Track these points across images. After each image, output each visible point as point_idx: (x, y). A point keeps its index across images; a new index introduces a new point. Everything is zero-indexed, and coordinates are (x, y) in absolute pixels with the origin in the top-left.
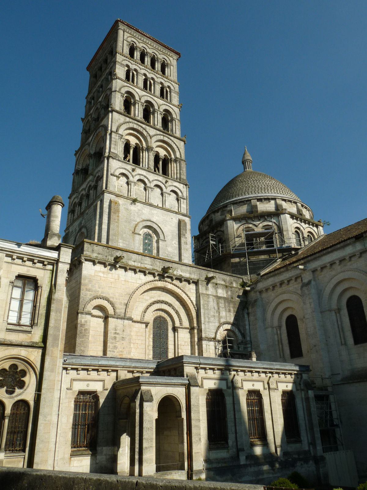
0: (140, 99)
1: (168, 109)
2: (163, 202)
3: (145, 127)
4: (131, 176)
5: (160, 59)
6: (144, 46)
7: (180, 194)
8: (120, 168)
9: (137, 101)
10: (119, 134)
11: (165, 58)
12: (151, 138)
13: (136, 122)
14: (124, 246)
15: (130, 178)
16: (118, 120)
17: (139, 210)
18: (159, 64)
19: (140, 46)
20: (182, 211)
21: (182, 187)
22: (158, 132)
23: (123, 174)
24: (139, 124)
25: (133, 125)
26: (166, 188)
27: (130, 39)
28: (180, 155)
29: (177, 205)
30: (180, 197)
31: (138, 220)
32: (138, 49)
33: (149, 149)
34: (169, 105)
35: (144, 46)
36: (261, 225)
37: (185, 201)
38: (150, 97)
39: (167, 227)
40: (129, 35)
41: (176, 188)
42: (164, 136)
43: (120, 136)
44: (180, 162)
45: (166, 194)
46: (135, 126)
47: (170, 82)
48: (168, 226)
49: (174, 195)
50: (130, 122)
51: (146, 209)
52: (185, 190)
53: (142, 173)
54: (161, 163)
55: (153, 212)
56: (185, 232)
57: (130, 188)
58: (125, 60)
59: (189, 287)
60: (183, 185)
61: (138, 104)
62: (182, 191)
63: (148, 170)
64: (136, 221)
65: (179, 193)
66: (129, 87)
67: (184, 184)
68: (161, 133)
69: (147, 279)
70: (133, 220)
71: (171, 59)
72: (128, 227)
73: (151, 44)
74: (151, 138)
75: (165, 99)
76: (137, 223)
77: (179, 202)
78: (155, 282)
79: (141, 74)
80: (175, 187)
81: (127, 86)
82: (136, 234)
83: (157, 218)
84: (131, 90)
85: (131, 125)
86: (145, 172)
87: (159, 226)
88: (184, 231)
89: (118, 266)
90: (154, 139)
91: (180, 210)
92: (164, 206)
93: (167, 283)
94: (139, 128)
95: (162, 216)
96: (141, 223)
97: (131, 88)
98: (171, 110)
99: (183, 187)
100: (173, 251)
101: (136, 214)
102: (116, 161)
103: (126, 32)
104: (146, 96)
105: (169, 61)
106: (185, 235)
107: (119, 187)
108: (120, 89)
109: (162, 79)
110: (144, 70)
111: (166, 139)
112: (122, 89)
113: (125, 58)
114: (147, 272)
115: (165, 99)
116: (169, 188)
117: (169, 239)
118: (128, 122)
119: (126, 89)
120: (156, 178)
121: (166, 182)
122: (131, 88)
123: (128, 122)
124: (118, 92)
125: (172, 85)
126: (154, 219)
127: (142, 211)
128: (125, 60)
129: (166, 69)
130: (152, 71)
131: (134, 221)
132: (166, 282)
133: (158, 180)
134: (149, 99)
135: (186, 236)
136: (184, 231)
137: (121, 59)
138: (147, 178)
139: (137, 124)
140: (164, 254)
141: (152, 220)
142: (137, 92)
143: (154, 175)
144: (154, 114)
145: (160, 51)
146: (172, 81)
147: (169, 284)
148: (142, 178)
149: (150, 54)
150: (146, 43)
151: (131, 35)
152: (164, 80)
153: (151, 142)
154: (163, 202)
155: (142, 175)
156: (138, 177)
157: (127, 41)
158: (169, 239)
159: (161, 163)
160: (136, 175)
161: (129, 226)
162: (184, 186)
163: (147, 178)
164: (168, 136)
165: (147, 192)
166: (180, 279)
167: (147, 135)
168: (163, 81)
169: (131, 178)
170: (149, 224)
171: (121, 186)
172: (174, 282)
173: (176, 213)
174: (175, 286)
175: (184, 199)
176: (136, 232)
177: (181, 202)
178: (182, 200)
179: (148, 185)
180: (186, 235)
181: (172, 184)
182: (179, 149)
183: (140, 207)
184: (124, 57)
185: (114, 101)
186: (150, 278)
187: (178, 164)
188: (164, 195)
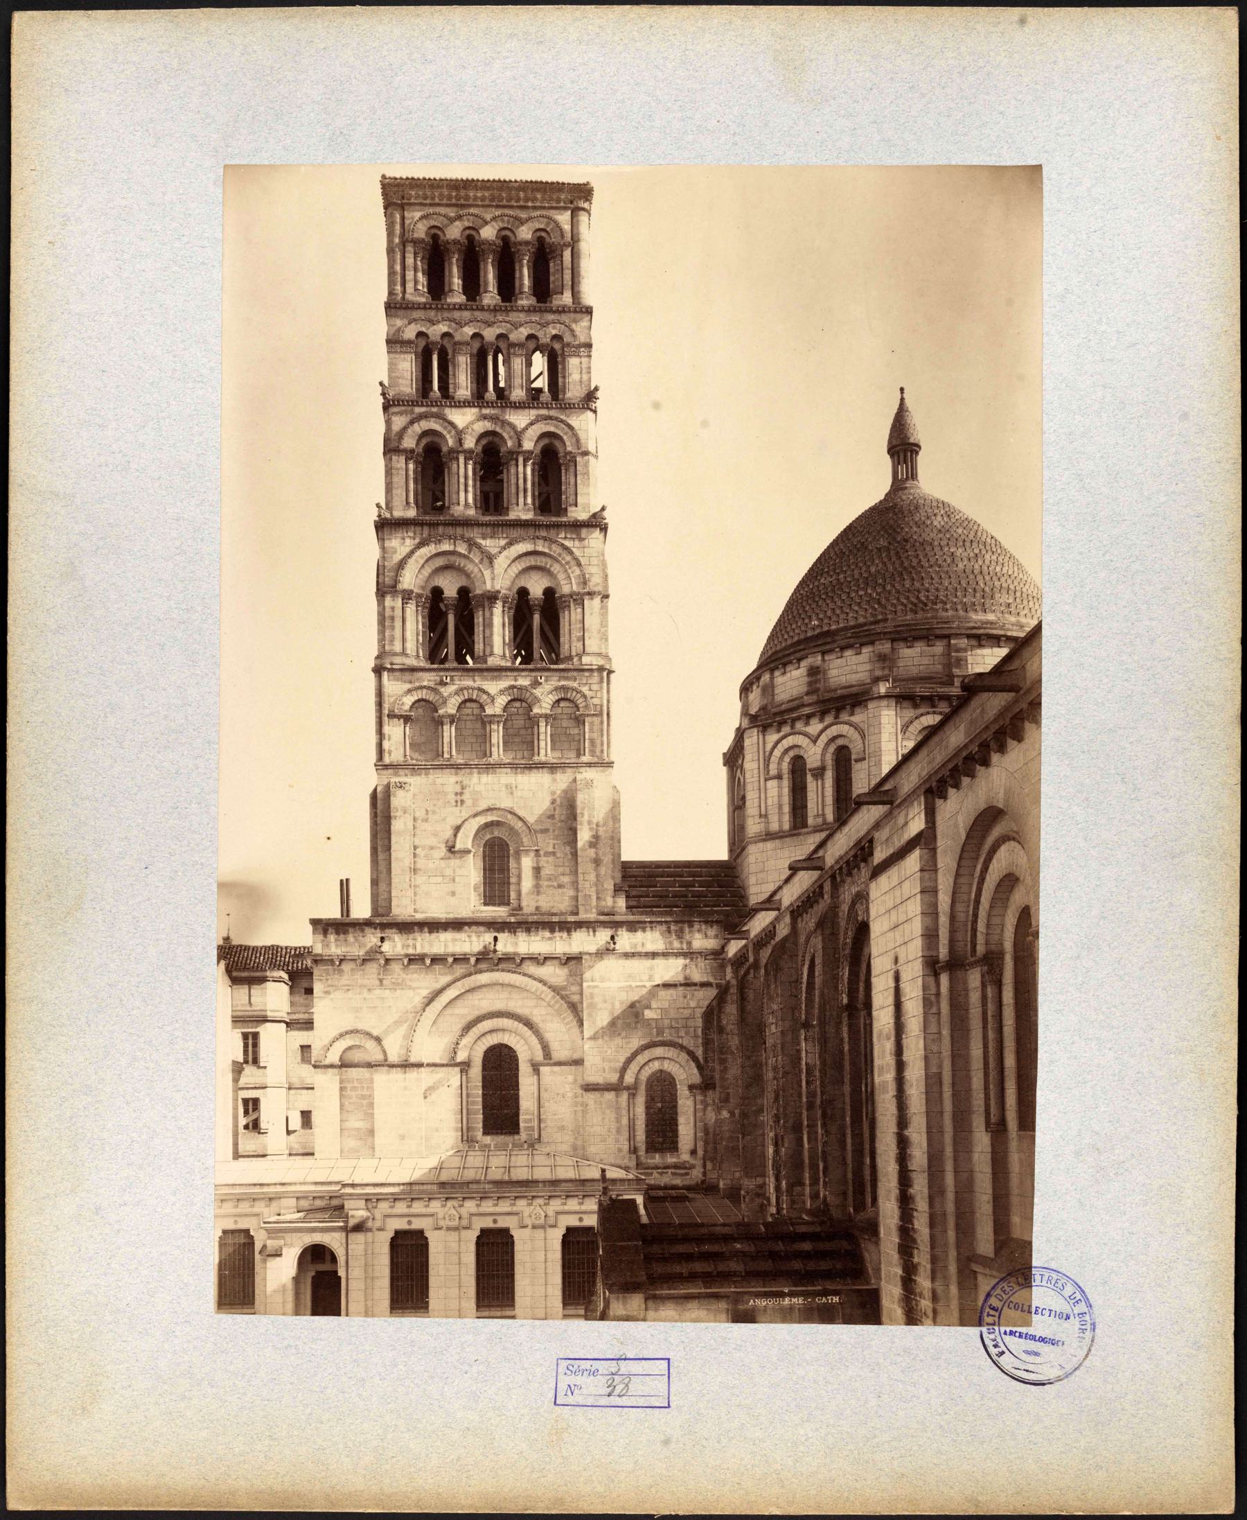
36: (824, 739)
119: (418, 428)
186: (459, 970)
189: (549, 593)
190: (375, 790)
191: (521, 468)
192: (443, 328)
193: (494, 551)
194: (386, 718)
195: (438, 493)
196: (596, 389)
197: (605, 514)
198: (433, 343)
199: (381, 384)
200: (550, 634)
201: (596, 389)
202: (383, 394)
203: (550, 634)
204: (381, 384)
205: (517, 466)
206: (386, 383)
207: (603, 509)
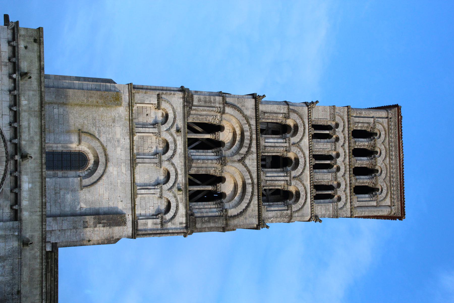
0: (294, 144)
1: (301, 196)
2: (145, 186)
3: (252, 152)
4: (169, 127)
5: (377, 181)
6: (383, 153)
7: (168, 216)
8: (173, 108)
9: (289, 140)
10: (224, 108)
11: (384, 190)
12: (239, 161)
13: (254, 136)
14: (55, 116)
15: (164, 125)
16: (244, 106)
17: (118, 141)
18: (369, 181)
19: (378, 145)
20: (140, 222)
21: (181, 221)
22: (255, 175)
23: (166, 117)
24: (254, 142)
25: (247, 131)
26: (169, 190)
27: (379, 127)
28: (233, 215)
29: (148, 213)
30: (162, 217)
31: (103, 139)
32: (372, 142)
33: (223, 161)
34: (309, 195)
35: (383, 153)
37: (159, 226)
38: (305, 161)
39: (105, 191)
40: (386, 125)
41: (175, 209)
42: (253, 183)
43: (222, 109)
44: (222, 216)
45: (159, 190)
46: (247, 134)
47: (349, 200)
48: (107, 193)
49: (163, 207)
50: (250, 125)
51: (123, 153)
52: (178, 226)
53: (178, 147)
54: (210, 188)
55: (122, 165)
56: (105, 223)
57: (149, 126)
58: (343, 119)
59: (6, 206)
60: (184, 221)
61: (286, 143)
62: (173, 221)
63: (188, 162)
64: (100, 136)
65: (168, 214)
66: (304, 125)
67: (186, 223)
68: (255, 181)
69: (5, 127)
70: (99, 130)
71: (388, 202)
72: (86, 122)
73: (392, 163)
74: (239, 161)
75: (315, 192)
76: (97, 137)
77: (155, 217)
78: (2, 141)
79: (335, 148)
80: (177, 207)
81: (303, 122)
82: (79, 136)
83: (115, 173)
84: (301, 129)
85: (246, 127)
86: (183, 152)
87: (102, 176)
88: (105, 221)
89: (14, 76)
90: (240, 166)
91: (140, 218)
92: (138, 188)
93: (4, 164)
94: (247, 142)
95: (122, 183)
96: (99, 144)
97: (304, 129)
98: (302, 201)
99: (181, 223)
100: (68, 203)
101: (110, 136)
102: (182, 103)
103: (388, 121)
104: (304, 154)
105: (382, 199)
106: (100, 223)
107: (144, 110)
108: (294, 111)
109: (346, 185)
110: (344, 152)
111: (249, 189)
112: (296, 115)
113: (346, 120)
114: (16, 125)
115: (315, 192)
116: (171, 194)
117: (85, 195)
118: (248, 122)
120: (179, 172)
121: (179, 190)
122: (304, 129)
123: (248, 122)
124: (289, 109)
125: (345, 204)
126: (111, 169)
127: (118, 146)
128: (343, 119)
129: (367, 196)
130: (349, 165)
131: (99, 132)
132: (6, 162)
133: (177, 174)
134: (301, 161)
135: (98, 225)
136: (105, 221)
137: (342, 114)
138: (173, 155)
139: (251, 137)
140: (58, 186)
141: (109, 164)
142: (301, 139)
143: (183, 167)
144: (283, 171)
145: (390, 181)
146: (351, 202)
147: (4, 168)
148: (172, 146)
149: (375, 163)
150: (389, 152)
151: (387, 129)
152: (346, 188)
153: (234, 161)
154: (145, 186)
155: (176, 145)
156: (170, 139)
157: (374, 123)
158: (85, 195)
159: (210, 188)
160: (172, 135)
161: (88, 124)
162: (184, 225)
163: (173, 155)
164: (256, 191)
165: (153, 157)
166: (17, 184)
167: (242, 154)
168: (343, 187)
169: (164, 128)
170: (102, 160)
171: (147, 115)
172: (8, 176)
173: (133, 209)
174: (3, 178)
175: (162, 224)
176: (83, 136)
177: (155, 220)
178: (159, 221)
179: (164, 157)
180: (101, 225)
181: (179, 201)
182: (241, 213)
183: (124, 142)
184: (348, 118)
185: (272, 103)
187: (217, 214)
188: (156, 187)
189: (222, 195)
190: (115, 83)
191: (282, 178)
192: (341, 136)
193: (247, 162)
194: (157, 93)
195: (265, 132)
196: (320, 221)
197: (265, 229)
198: (335, 131)
199: (317, 102)
200: (200, 196)
201: (320, 221)
202: (312, 103)
203: (200, 196)
204: (317, 102)
205: (284, 176)
206: (318, 104)
207: (267, 227)
